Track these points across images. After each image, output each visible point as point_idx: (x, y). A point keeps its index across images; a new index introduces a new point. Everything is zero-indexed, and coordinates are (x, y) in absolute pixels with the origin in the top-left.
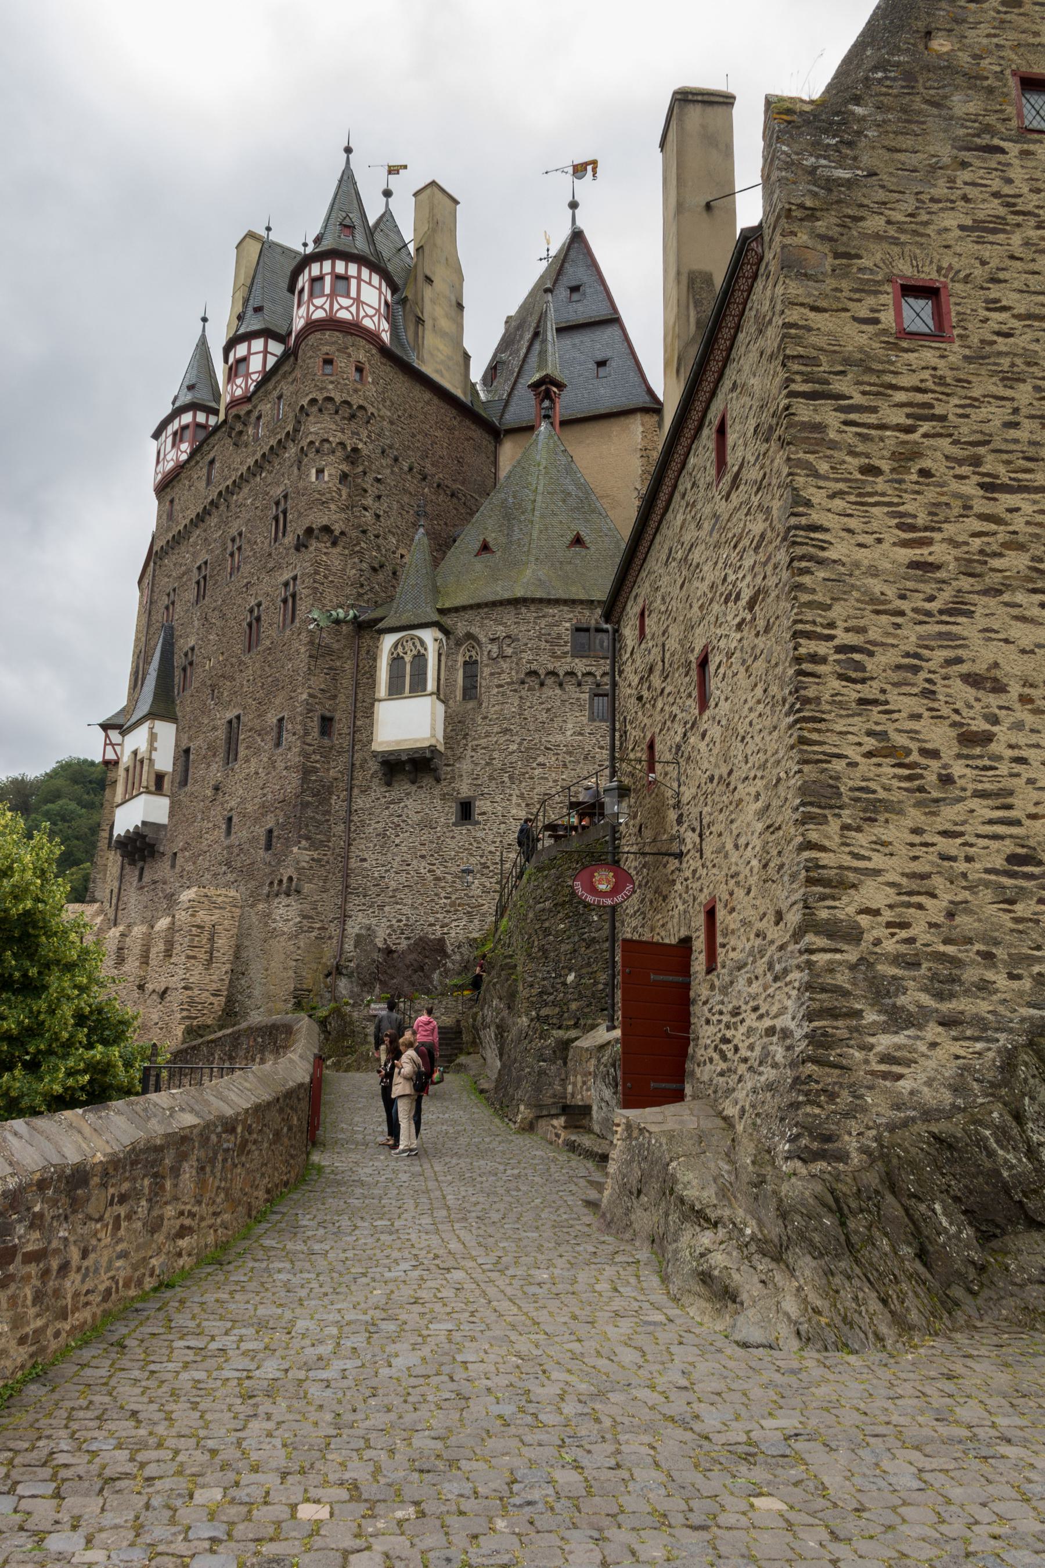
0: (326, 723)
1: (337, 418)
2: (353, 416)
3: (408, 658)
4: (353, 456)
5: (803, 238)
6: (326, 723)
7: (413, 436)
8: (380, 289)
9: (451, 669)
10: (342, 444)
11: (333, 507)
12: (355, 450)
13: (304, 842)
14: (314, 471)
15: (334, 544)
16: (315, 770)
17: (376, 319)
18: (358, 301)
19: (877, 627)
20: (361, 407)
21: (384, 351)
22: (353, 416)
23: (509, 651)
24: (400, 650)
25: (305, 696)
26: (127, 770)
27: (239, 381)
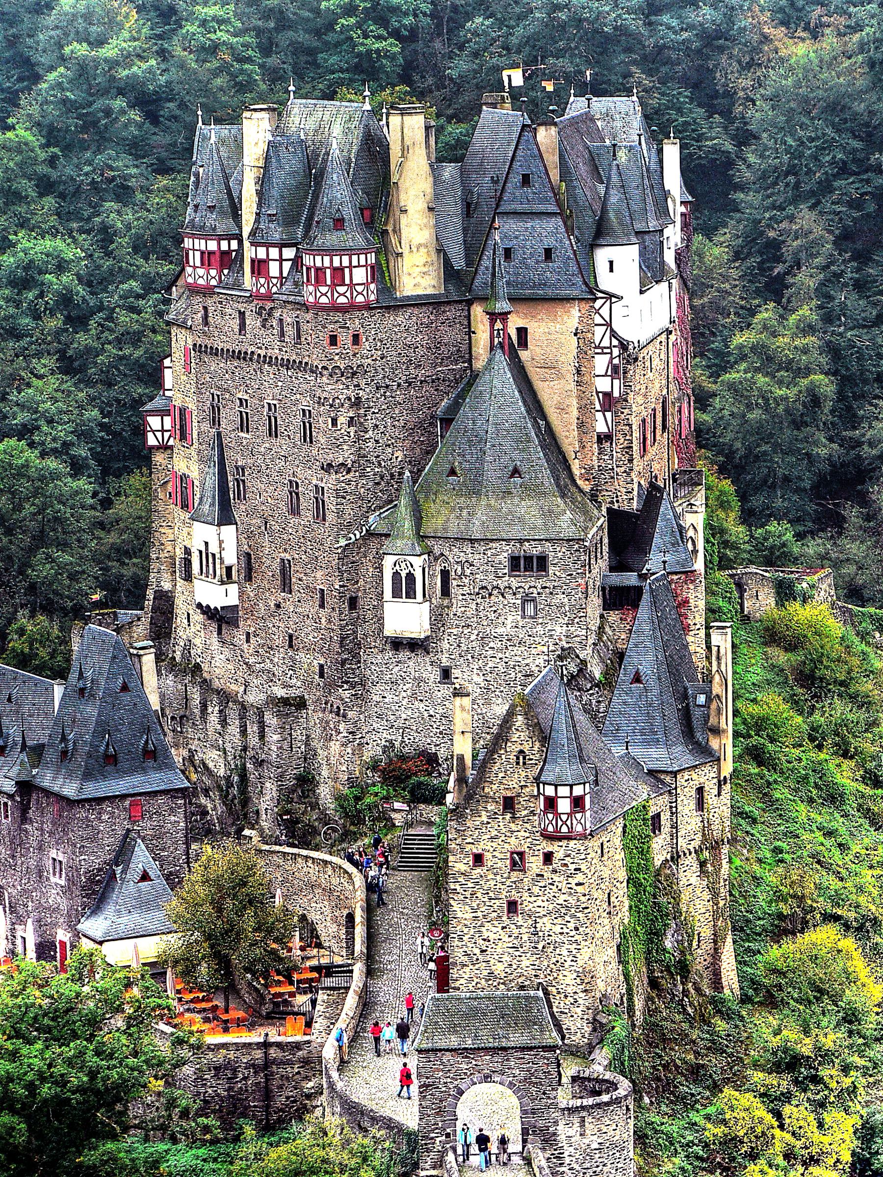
0: (353, 603)
3: (403, 575)
4: (357, 403)
5: (453, 846)
6: (353, 603)
8: (366, 266)
9: (432, 576)
11: (345, 447)
12: (358, 398)
13: (346, 687)
14: (330, 420)
15: (348, 473)
16: (348, 636)
18: (352, 286)
19: (466, 930)
23: (468, 572)
24: (397, 567)
25: (337, 587)
26: (201, 552)
27: (262, 280)
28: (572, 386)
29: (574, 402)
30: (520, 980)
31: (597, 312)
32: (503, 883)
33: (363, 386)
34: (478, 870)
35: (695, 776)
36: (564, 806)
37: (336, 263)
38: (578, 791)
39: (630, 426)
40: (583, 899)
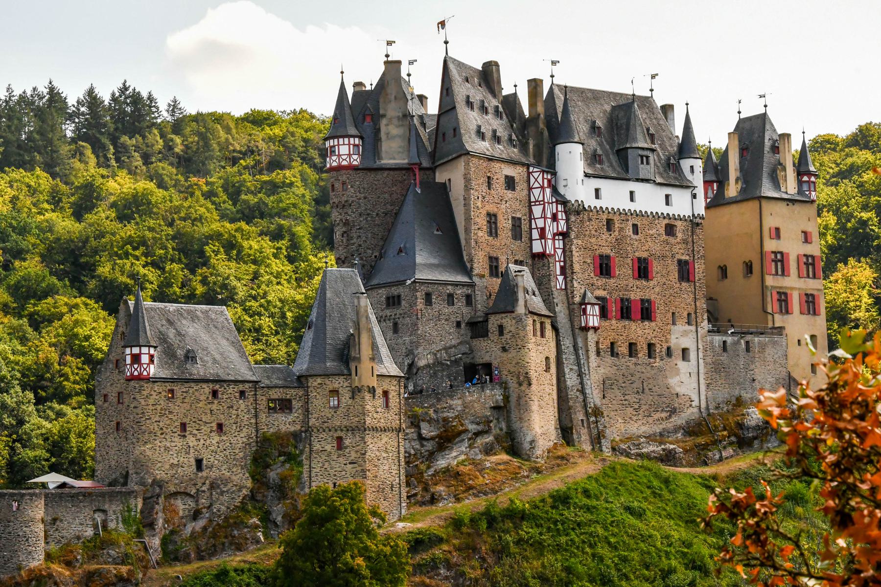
1: (338, 209)
2: (344, 206)
4: (346, 223)
7: (379, 197)
8: (349, 144)
10: (341, 220)
11: (340, 248)
17: (348, 159)
18: (339, 155)
20: (347, 201)
21: (355, 169)
22: (344, 206)
28: (463, 208)
29: (463, 216)
30: (121, 470)
31: (536, 180)
32: (115, 411)
33: (350, 213)
34: (106, 405)
35: (327, 382)
36: (128, 360)
37: (332, 144)
38: (136, 350)
39: (572, 252)
40: (136, 416)
